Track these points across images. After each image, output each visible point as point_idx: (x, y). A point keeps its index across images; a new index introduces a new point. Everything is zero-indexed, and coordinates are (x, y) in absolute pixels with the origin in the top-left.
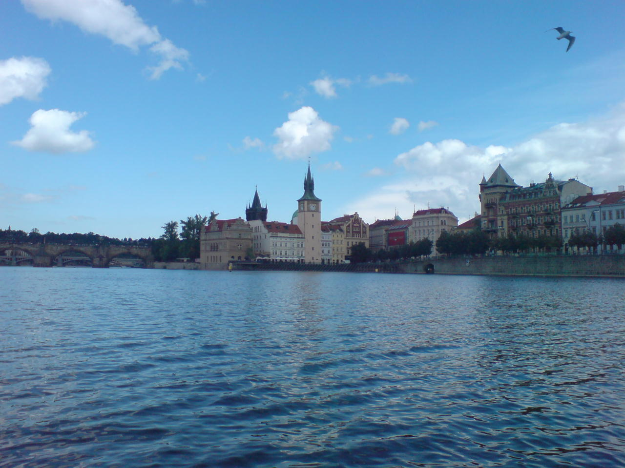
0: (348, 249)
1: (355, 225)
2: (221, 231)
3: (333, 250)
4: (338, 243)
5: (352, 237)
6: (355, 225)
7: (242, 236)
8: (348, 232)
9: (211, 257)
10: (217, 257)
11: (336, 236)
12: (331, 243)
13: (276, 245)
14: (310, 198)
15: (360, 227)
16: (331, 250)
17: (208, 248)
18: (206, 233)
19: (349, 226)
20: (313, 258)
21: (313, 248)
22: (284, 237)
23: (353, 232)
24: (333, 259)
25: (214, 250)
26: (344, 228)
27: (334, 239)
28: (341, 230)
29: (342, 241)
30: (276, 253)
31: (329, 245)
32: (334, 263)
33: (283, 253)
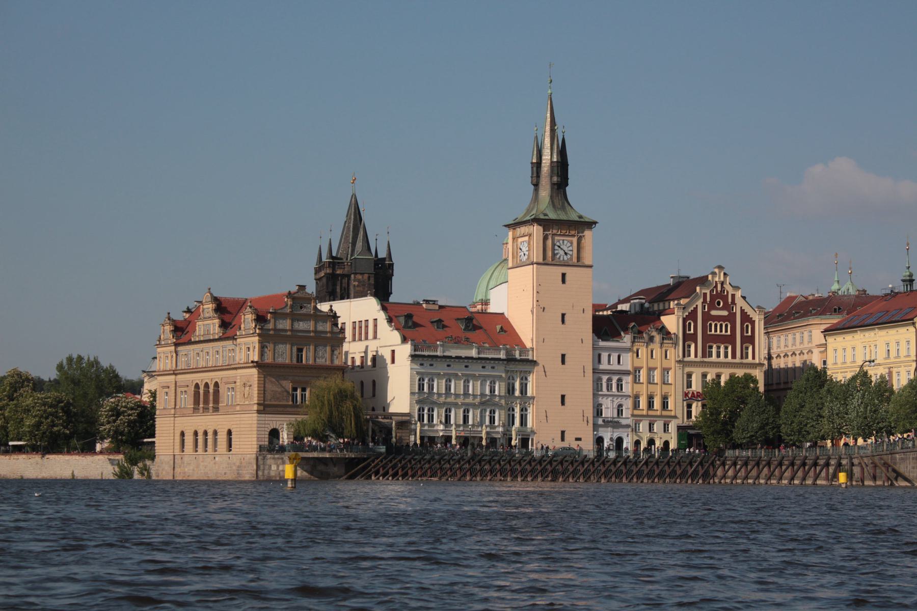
0: (690, 398)
1: (714, 313)
2: (233, 338)
3: (636, 405)
5: (704, 356)
6: (714, 313)
7: (308, 357)
8: (689, 338)
9: (196, 434)
10: (215, 433)
11: (643, 351)
13: (431, 387)
14: (552, 215)
15: (731, 318)
16: (628, 404)
17: (187, 400)
18: (176, 345)
19: (693, 315)
23: (707, 339)
25: (206, 409)
26: (672, 322)
27: (637, 363)
28: (665, 333)
29: (666, 370)
31: (620, 387)
33: (456, 416)
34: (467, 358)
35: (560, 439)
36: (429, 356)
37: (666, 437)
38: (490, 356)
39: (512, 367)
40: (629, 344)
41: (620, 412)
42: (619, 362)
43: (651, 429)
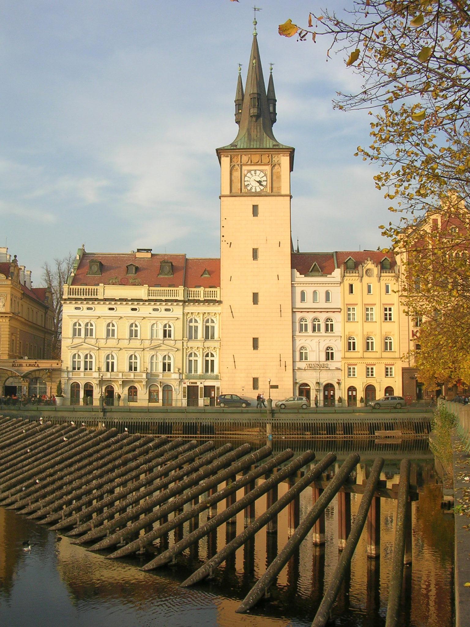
3: (351, 346)
4: (367, 318)
12: (338, 320)
13: (89, 332)
20: (255, 381)
22: (121, 300)
24: (349, 382)
31: (329, 328)
32: (352, 399)
34: (132, 300)
35: (252, 386)
37: (388, 382)
40: (339, 279)
41: (329, 356)
42: (328, 299)
43: (369, 372)
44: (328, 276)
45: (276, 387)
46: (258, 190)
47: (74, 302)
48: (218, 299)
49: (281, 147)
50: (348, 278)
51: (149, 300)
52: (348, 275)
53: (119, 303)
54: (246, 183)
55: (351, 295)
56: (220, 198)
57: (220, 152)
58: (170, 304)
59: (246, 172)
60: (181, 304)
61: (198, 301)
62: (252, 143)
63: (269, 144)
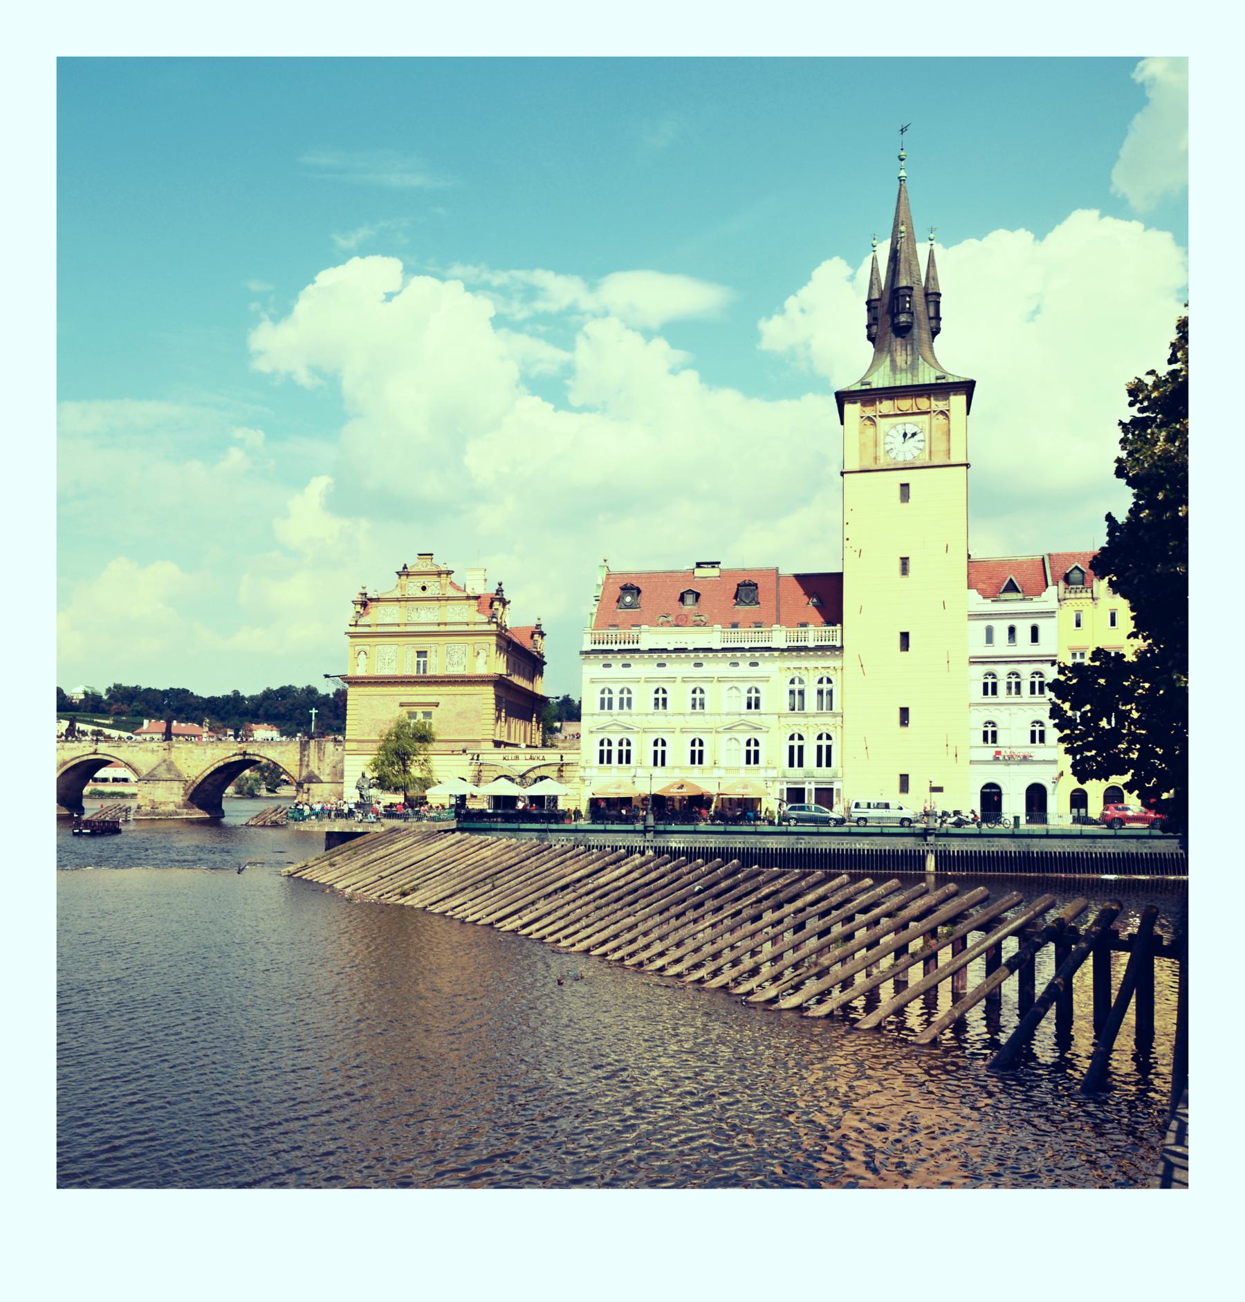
7: (436, 667)
20: (904, 781)
21: (904, 712)
22: (677, 650)
30: (625, 757)
33: (678, 752)
36: (620, 651)
38: (747, 646)
39: (794, 662)
40: (1052, 604)
42: (1035, 638)
44: (1035, 599)
45: (940, 789)
46: (909, 458)
47: (601, 656)
48: (838, 644)
49: (951, 380)
50: (1073, 602)
51: (724, 650)
52: (1073, 596)
53: (674, 655)
54: (888, 447)
55: (905, 579)
56: (842, 474)
57: (842, 398)
58: (757, 654)
59: (887, 428)
60: (776, 654)
61: (806, 649)
62: (898, 376)
63: (927, 376)
